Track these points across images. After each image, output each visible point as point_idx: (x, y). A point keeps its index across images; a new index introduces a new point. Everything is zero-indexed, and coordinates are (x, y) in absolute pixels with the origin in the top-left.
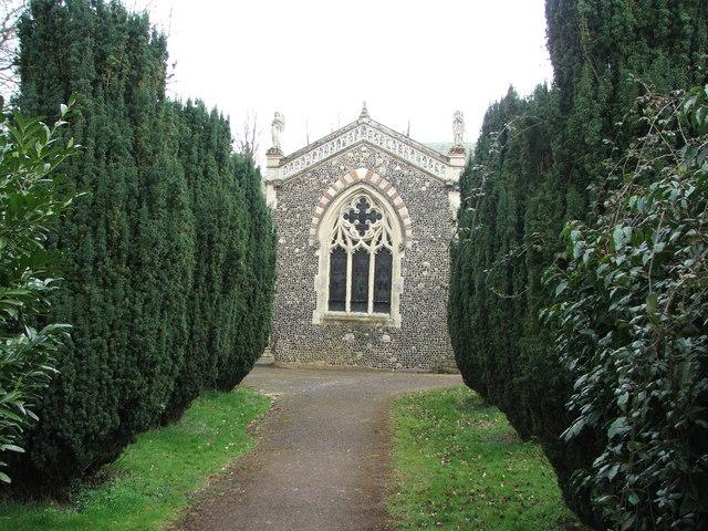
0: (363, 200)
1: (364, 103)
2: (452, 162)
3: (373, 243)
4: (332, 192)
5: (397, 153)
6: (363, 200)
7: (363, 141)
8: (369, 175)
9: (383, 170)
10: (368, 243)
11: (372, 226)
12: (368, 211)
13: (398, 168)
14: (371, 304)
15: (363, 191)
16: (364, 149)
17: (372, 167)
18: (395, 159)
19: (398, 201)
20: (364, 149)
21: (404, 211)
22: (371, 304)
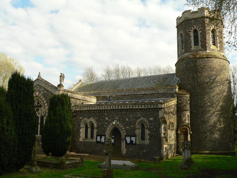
0: (38, 101)
1: (39, 73)
2: (58, 89)
3: (40, 114)
4: (43, 99)
5: (45, 87)
6: (38, 101)
7: (38, 84)
8: (39, 94)
9: (42, 92)
10: (39, 114)
11: (40, 109)
12: (39, 105)
13: (45, 92)
14: (39, 133)
15: (38, 99)
16: (38, 86)
17: (40, 92)
18: (45, 89)
19: (45, 101)
20: (38, 86)
21: (46, 104)
22: (39, 133)
